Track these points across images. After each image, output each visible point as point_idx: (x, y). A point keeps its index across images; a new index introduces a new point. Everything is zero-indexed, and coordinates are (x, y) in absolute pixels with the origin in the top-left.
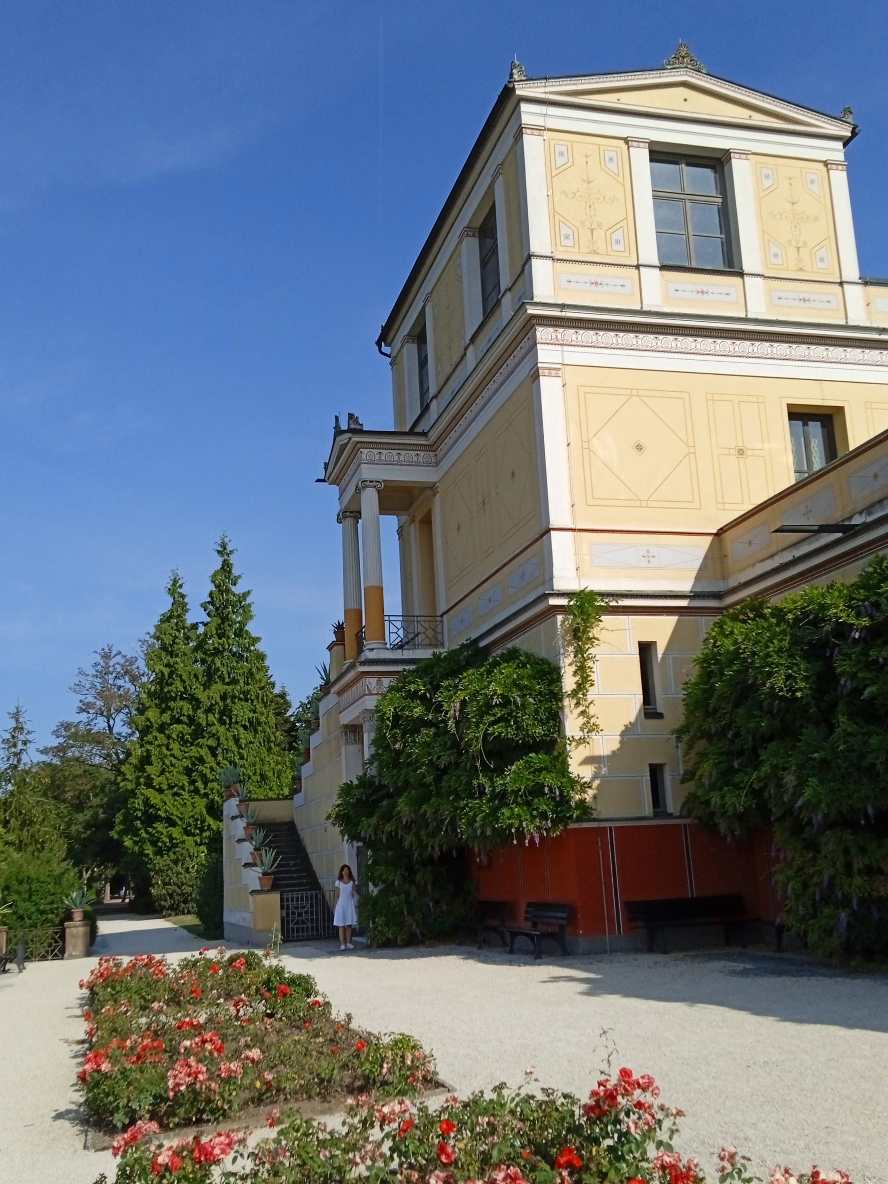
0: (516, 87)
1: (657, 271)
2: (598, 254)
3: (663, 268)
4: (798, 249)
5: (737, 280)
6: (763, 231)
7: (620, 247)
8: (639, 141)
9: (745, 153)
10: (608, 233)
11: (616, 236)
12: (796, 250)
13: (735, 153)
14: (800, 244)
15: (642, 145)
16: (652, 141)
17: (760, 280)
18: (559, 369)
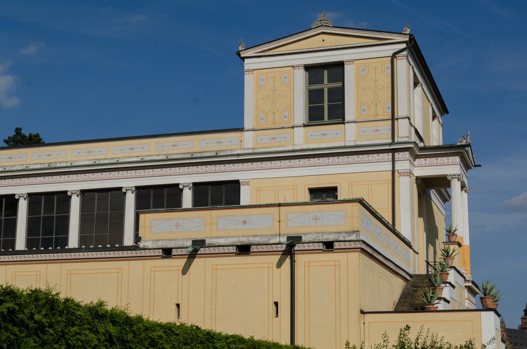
0: (241, 53)
1: (302, 128)
2: (276, 124)
3: (305, 126)
4: (376, 105)
5: (342, 125)
6: (358, 99)
7: (287, 119)
8: (298, 66)
9: (352, 61)
10: (281, 114)
11: (284, 114)
12: (375, 105)
13: (346, 62)
14: (378, 102)
15: (300, 68)
16: (304, 65)
17: (353, 124)
18: (249, 182)
